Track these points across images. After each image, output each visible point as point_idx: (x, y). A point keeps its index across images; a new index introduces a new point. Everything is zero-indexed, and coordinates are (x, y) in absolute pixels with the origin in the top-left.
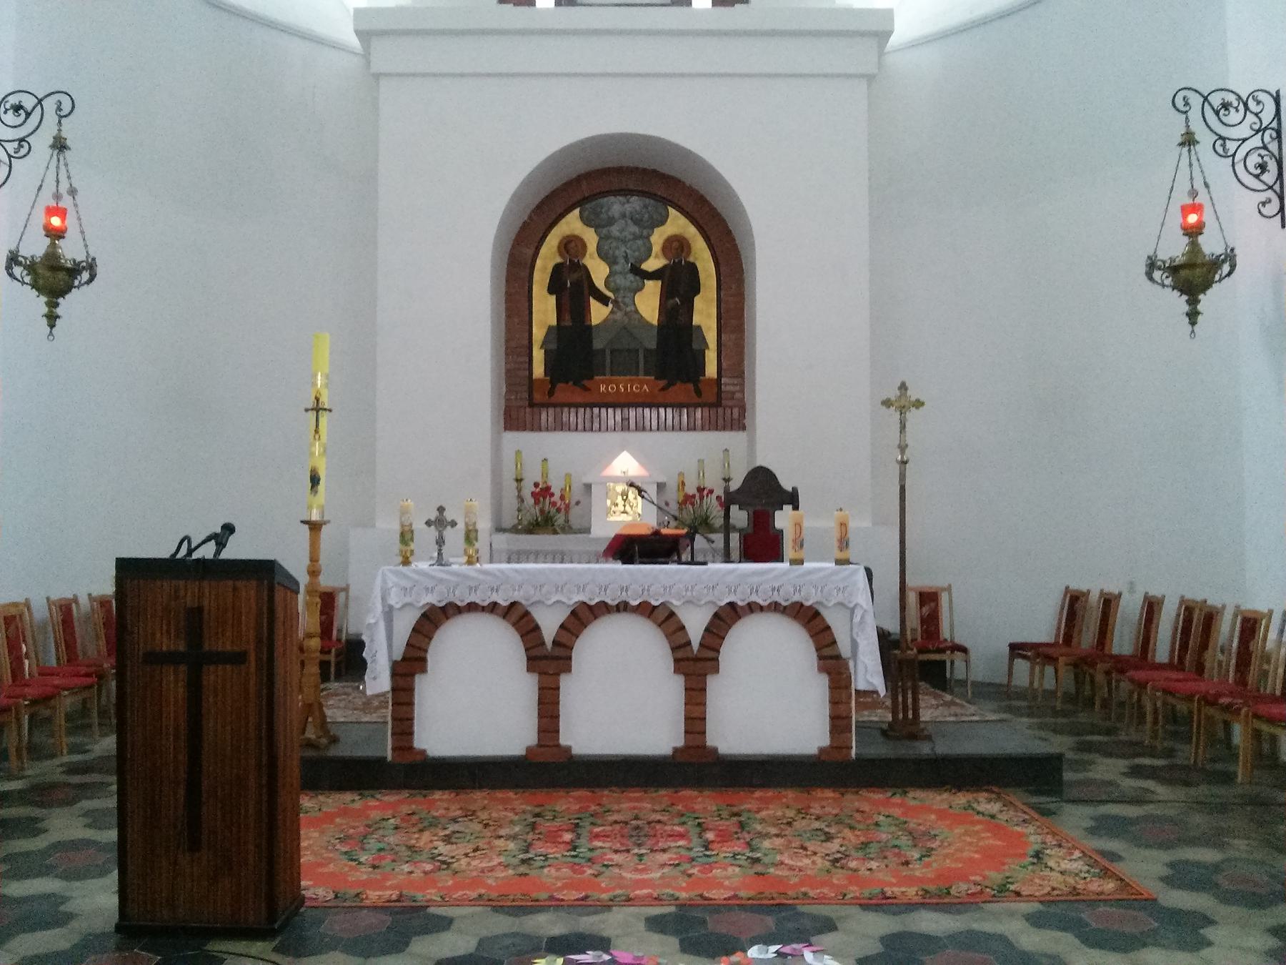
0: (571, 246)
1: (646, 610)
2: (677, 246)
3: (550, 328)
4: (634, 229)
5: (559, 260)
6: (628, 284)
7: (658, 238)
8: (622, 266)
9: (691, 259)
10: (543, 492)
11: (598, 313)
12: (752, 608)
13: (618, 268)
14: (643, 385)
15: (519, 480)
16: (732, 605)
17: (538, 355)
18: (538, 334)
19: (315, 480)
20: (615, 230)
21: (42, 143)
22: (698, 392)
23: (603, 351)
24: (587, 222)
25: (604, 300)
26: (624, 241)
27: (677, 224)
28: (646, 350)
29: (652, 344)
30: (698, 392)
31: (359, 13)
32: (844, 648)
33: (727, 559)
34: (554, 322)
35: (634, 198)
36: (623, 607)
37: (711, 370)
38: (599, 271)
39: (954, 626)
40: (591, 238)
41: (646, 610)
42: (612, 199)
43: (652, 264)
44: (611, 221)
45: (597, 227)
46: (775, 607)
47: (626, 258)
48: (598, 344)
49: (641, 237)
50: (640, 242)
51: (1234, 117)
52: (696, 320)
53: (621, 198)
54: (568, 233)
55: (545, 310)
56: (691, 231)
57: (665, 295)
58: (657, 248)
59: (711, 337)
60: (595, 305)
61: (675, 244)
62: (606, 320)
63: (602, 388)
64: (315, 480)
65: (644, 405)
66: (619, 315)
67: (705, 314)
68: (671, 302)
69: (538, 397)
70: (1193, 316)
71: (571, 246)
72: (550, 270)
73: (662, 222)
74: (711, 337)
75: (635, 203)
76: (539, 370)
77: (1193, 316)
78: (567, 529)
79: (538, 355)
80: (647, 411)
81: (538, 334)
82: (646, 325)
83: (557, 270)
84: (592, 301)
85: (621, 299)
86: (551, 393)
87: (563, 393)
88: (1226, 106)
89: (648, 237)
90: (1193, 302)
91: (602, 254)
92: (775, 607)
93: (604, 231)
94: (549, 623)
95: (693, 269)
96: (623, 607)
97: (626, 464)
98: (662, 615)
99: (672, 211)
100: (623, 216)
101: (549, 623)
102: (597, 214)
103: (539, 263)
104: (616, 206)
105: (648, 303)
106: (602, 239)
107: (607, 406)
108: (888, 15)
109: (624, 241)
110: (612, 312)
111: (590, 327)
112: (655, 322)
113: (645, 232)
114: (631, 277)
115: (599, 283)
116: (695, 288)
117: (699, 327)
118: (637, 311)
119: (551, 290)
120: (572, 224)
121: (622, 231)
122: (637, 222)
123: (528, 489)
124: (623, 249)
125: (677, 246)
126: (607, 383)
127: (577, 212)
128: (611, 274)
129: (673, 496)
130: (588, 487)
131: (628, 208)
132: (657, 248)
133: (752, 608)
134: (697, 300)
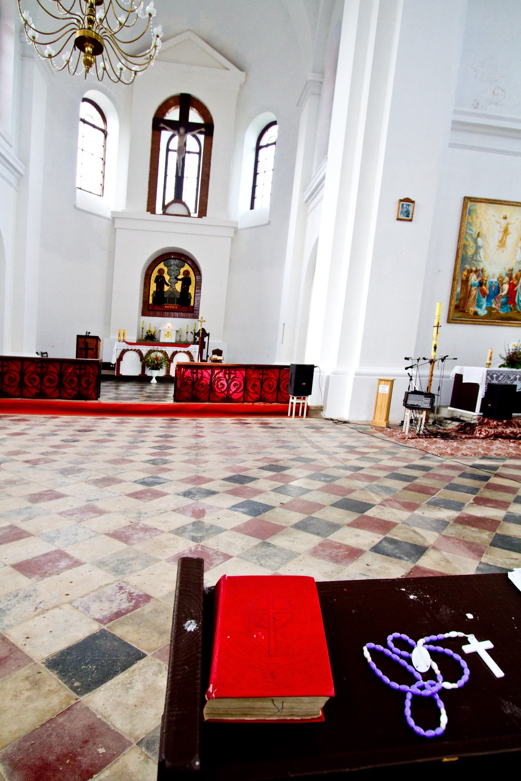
0: (161, 271)
2: (186, 273)
3: (154, 292)
5: (158, 274)
6: (174, 281)
7: (182, 270)
9: (190, 276)
11: (166, 288)
13: (172, 277)
15: (143, 328)
16: (176, 351)
18: (151, 293)
20: (172, 268)
23: (167, 297)
24: (165, 265)
25: (168, 285)
26: (174, 271)
27: (187, 267)
28: (177, 298)
29: (178, 297)
34: (155, 290)
35: (177, 260)
38: (167, 278)
40: (166, 269)
42: (172, 260)
43: (181, 277)
44: (171, 266)
45: (168, 267)
47: (174, 275)
48: (166, 296)
49: (178, 270)
50: (177, 271)
52: (190, 291)
53: (174, 260)
54: (160, 268)
55: (153, 287)
56: (190, 270)
60: (165, 286)
61: (186, 272)
62: (168, 290)
63: (166, 307)
65: (175, 312)
66: (171, 289)
68: (184, 287)
69: (150, 308)
71: (161, 271)
72: (155, 277)
73: (183, 266)
74: (193, 296)
75: (177, 262)
76: (151, 302)
80: (176, 313)
81: (151, 293)
82: (177, 292)
83: (157, 276)
84: (165, 285)
85: (172, 285)
86: (153, 307)
87: (156, 308)
89: (180, 270)
91: (168, 274)
93: (169, 268)
95: (190, 279)
98: (164, 352)
99: (186, 264)
100: (174, 265)
102: (168, 264)
103: (153, 275)
104: (173, 262)
105: (178, 286)
106: (169, 270)
107: (167, 311)
109: (174, 271)
110: (170, 288)
111: (164, 292)
112: (180, 291)
113: (179, 269)
114: (175, 280)
115: (167, 281)
116: (190, 284)
117: (190, 293)
118: (175, 288)
119: (155, 282)
120: (161, 266)
121: (173, 268)
122: (177, 266)
124: (173, 273)
125: (186, 273)
126: (167, 306)
127: (163, 262)
128: (170, 279)
130: (160, 330)
131: (175, 263)
134: (190, 286)
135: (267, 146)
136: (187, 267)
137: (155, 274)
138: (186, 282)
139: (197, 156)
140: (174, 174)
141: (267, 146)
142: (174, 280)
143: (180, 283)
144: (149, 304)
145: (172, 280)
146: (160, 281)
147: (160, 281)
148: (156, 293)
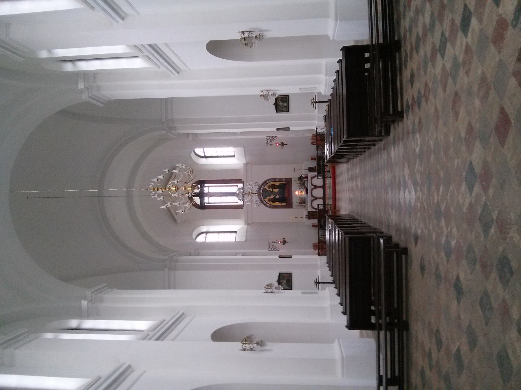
0: (269, 200)
1: (312, 191)
4: (267, 192)
7: (268, 189)
8: (271, 194)
10: (300, 203)
11: (277, 197)
12: (311, 183)
14: (286, 191)
15: (299, 206)
17: (283, 204)
18: (280, 204)
19: (302, 218)
21: (272, 244)
22: (287, 184)
25: (276, 196)
29: (281, 190)
30: (287, 184)
31: (245, 225)
32: (314, 176)
33: (307, 180)
34: (279, 202)
36: (311, 193)
37: (284, 182)
38: (272, 197)
39: (314, 155)
40: (268, 198)
41: (312, 191)
43: (271, 190)
46: (311, 181)
48: (281, 197)
49: (268, 192)
51: (268, 141)
55: (277, 203)
57: (275, 188)
58: (269, 189)
59: (281, 182)
60: (276, 197)
64: (302, 218)
67: (277, 183)
70: (286, 144)
71: (269, 200)
74: (281, 182)
76: (285, 204)
77: (286, 144)
78: (305, 200)
79: (283, 204)
81: (280, 204)
82: (279, 191)
84: (276, 197)
85: (276, 193)
86: (287, 202)
88: (267, 141)
90: (285, 145)
91: (270, 196)
92: (311, 181)
94: (313, 198)
96: (311, 193)
97: (297, 193)
101: (313, 198)
105: (276, 190)
108: (244, 163)
115: (274, 196)
116: (274, 184)
117: (279, 184)
119: (275, 202)
123: (300, 205)
125: (269, 187)
129: (300, 187)
130: (300, 197)
132: (269, 189)
133: (311, 183)
135: (204, 152)
136: (266, 187)
137: (271, 203)
138: (273, 186)
139: (210, 188)
140: (219, 198)
141: (204, 152)
142: (273, 193)
143: (274, 190)
144: (286, 205)
145: (273, 194)
146: (274, 200)
147: (274, 200)
148: (280, 202)
